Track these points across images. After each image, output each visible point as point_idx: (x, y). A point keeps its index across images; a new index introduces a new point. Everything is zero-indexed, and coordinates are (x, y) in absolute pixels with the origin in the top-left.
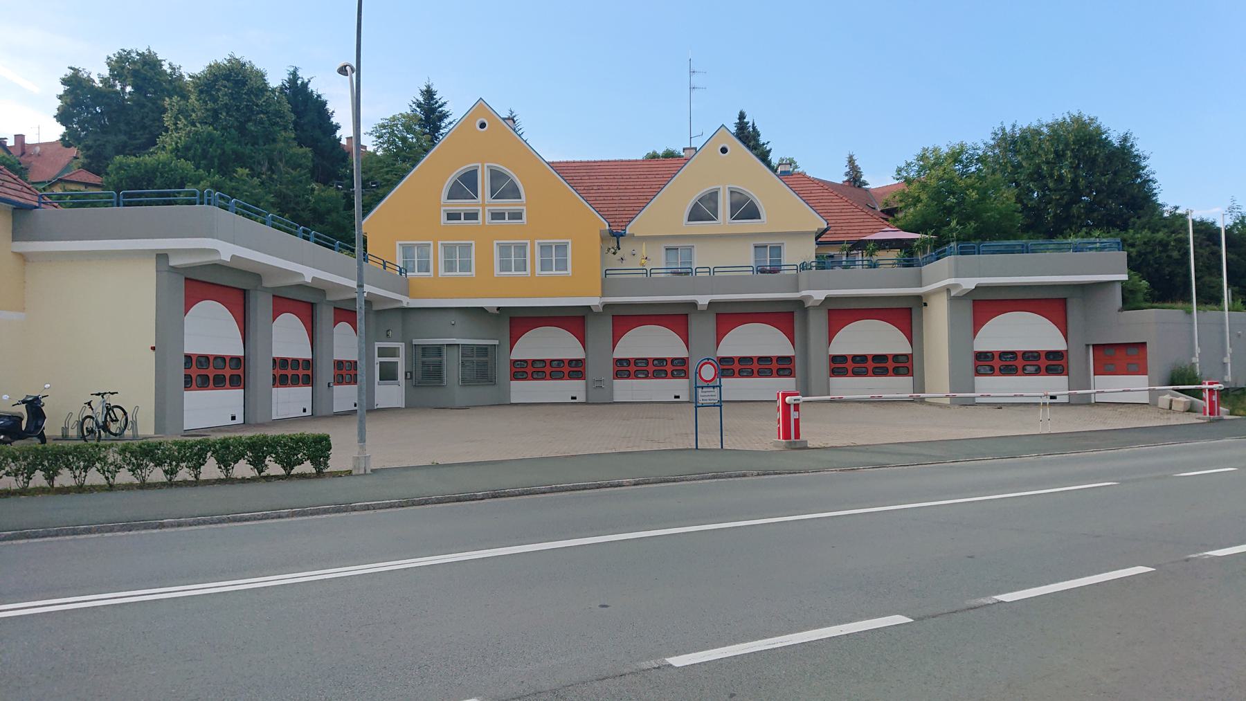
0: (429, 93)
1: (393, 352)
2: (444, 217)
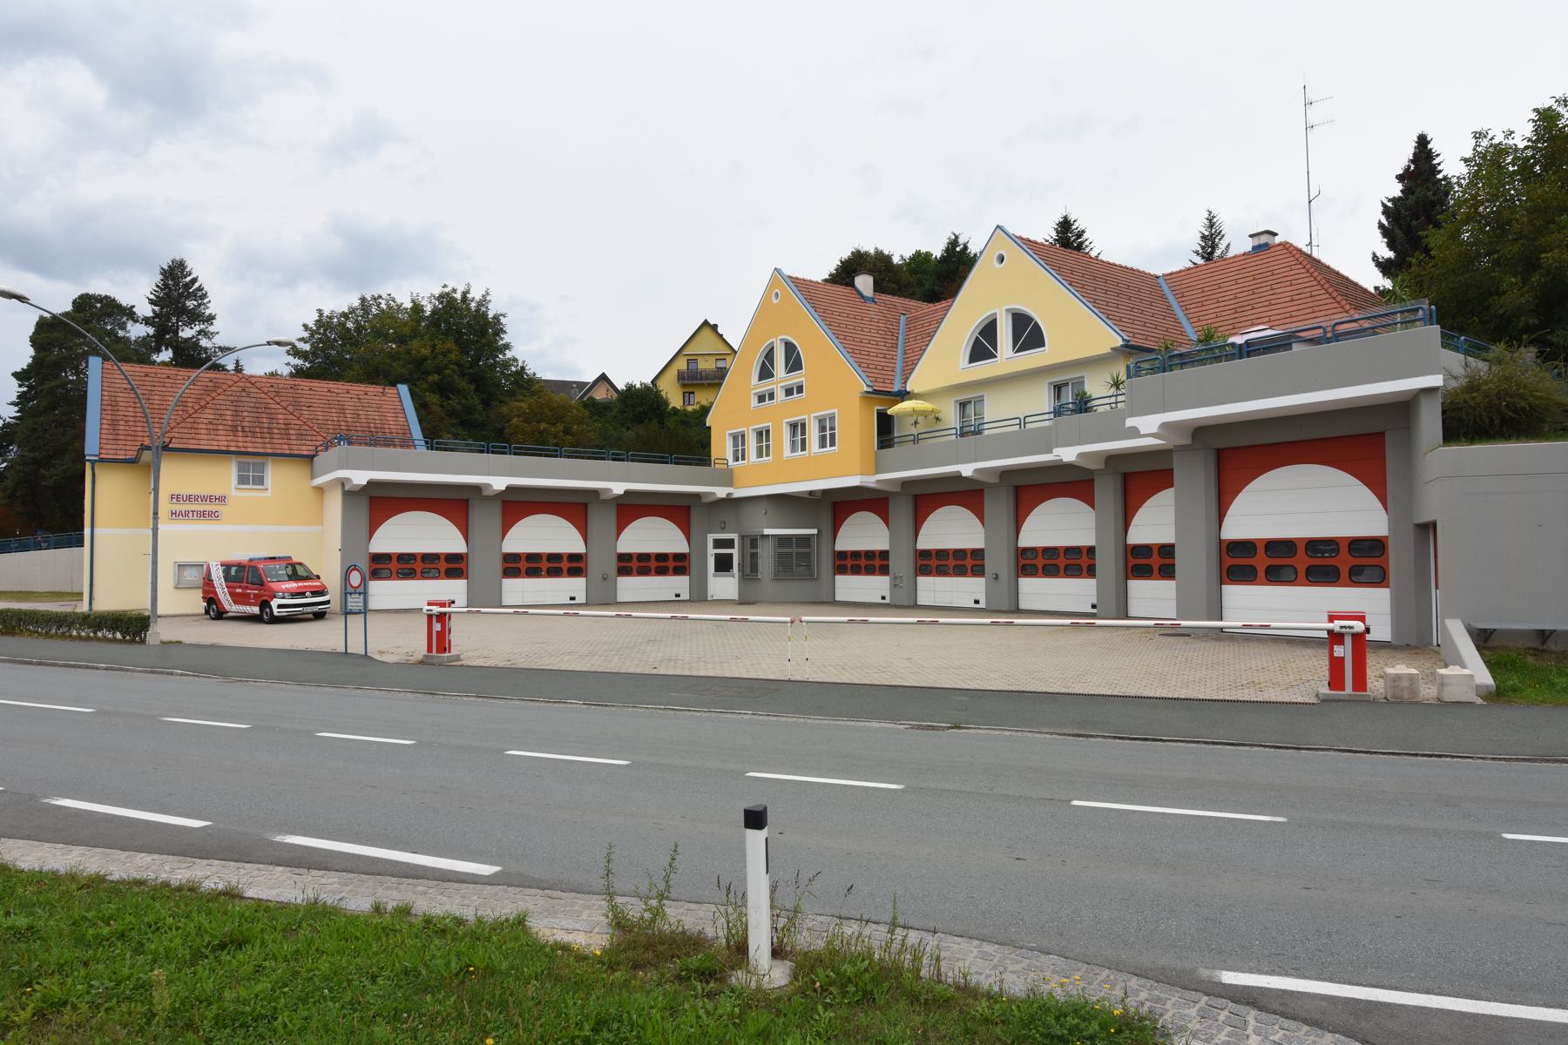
1: (729, 543)
2: (754, 402)
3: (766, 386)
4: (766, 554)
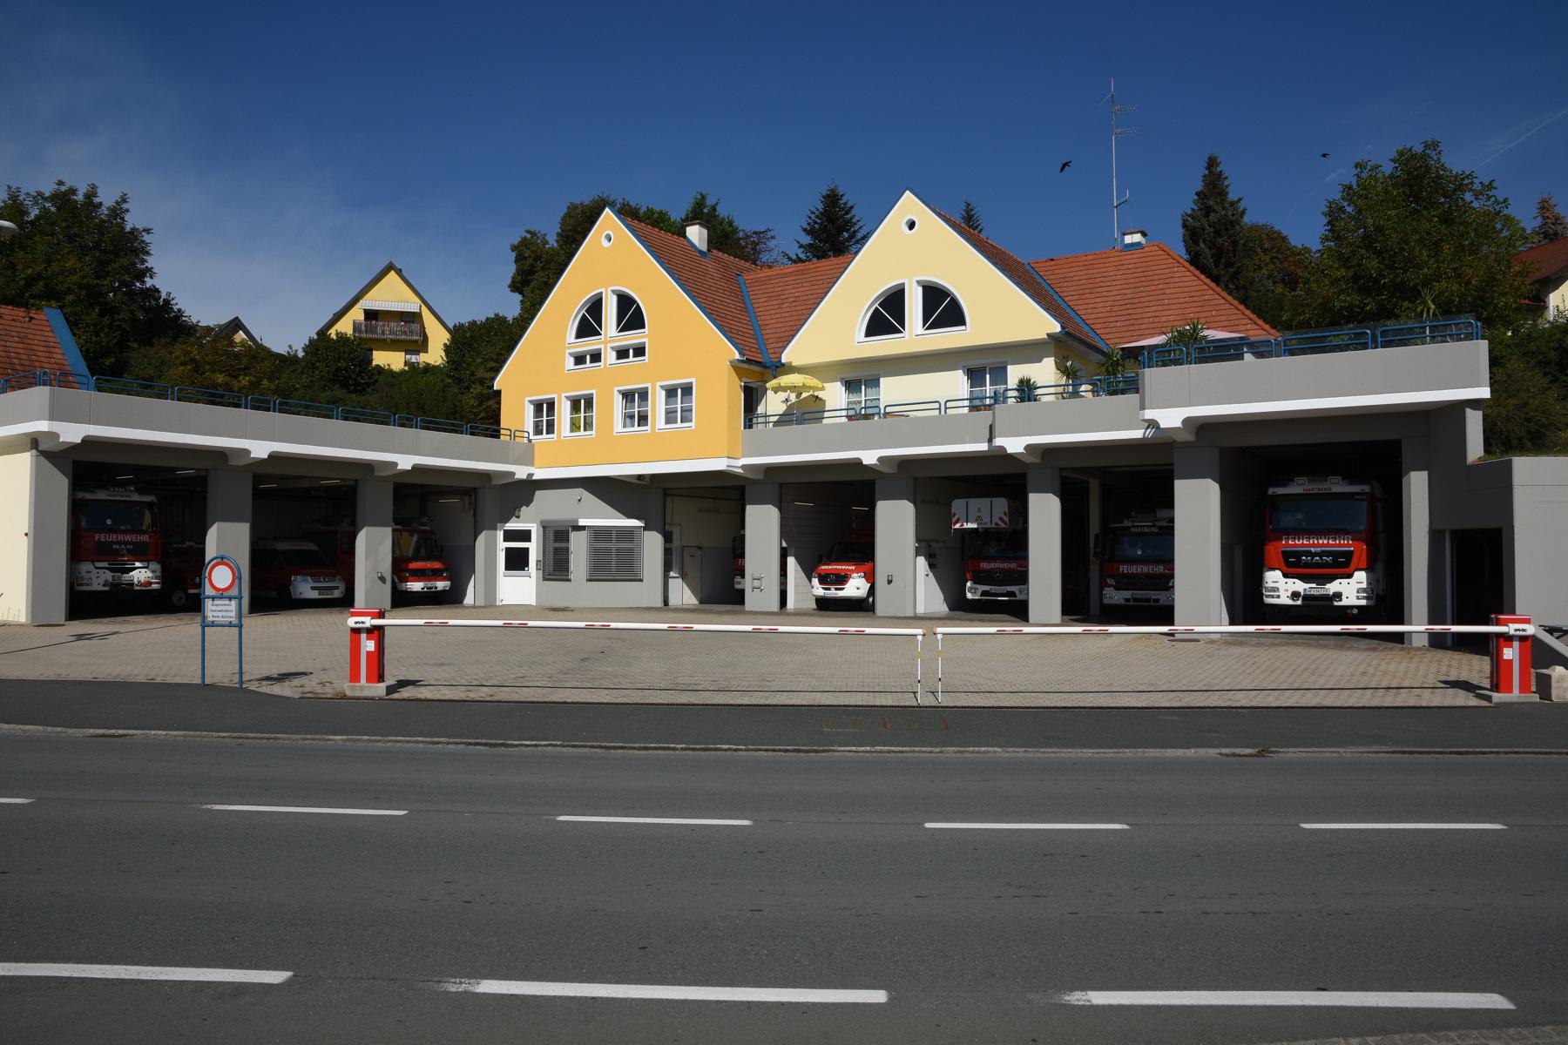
0: (832, 199)
1: (525, 536)
3: (589, 344)
4: (579, 546)
